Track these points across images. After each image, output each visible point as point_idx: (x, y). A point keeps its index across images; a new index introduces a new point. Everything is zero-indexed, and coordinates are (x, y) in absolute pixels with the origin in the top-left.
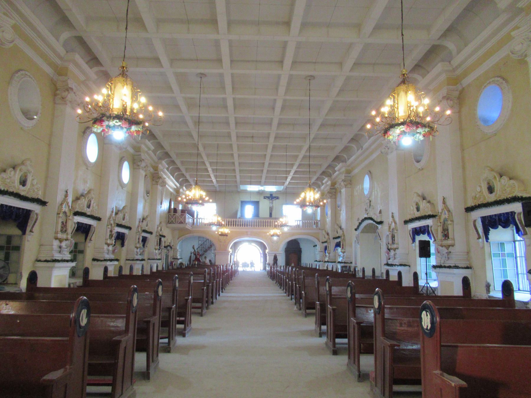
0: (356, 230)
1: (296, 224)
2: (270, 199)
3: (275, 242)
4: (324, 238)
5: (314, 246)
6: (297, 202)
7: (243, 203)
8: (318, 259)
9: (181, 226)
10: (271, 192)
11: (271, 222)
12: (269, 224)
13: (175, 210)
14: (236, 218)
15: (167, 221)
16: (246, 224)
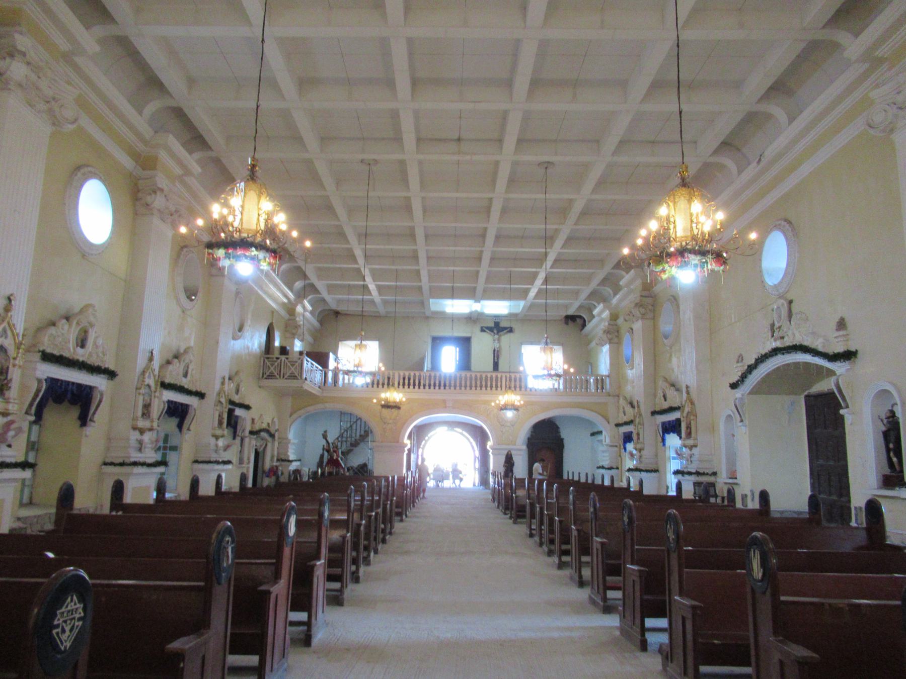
0: (734, 386)
1: (551, 387)
2: (495, 331)
3: (509, 424)
4: (622, 414)
5: (593, 434)
6: (642, 238)
7: (437, 341)
8: (606, 464)
9: (293, 383)
10: (496, 316)
11: (499, 379)
12: (494, 384)
13: (284, 351)
14: (422, 369)
16: (441, 384)
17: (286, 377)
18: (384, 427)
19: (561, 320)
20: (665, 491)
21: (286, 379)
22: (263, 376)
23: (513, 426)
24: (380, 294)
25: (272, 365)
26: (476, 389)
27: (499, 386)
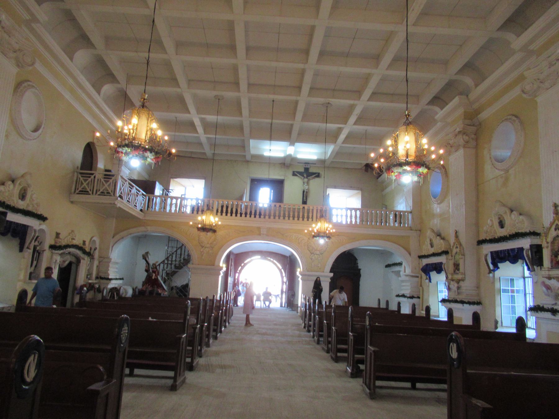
2: (305, 175)
3: (318, 252)
5: (388, 266)
8: (407, 292)
12: (306, 215)
15: (73, 191)
16: (256, 213)
17: (98, 193)
18: (202, 250)
19: (361, 169)
20: (493, 327)
21: (99, 195)
22: (75, 192)
23: (322, 254)
24: (205, 132)
25: (85, 180)
26: (289, 219)
27: (310, 217)
